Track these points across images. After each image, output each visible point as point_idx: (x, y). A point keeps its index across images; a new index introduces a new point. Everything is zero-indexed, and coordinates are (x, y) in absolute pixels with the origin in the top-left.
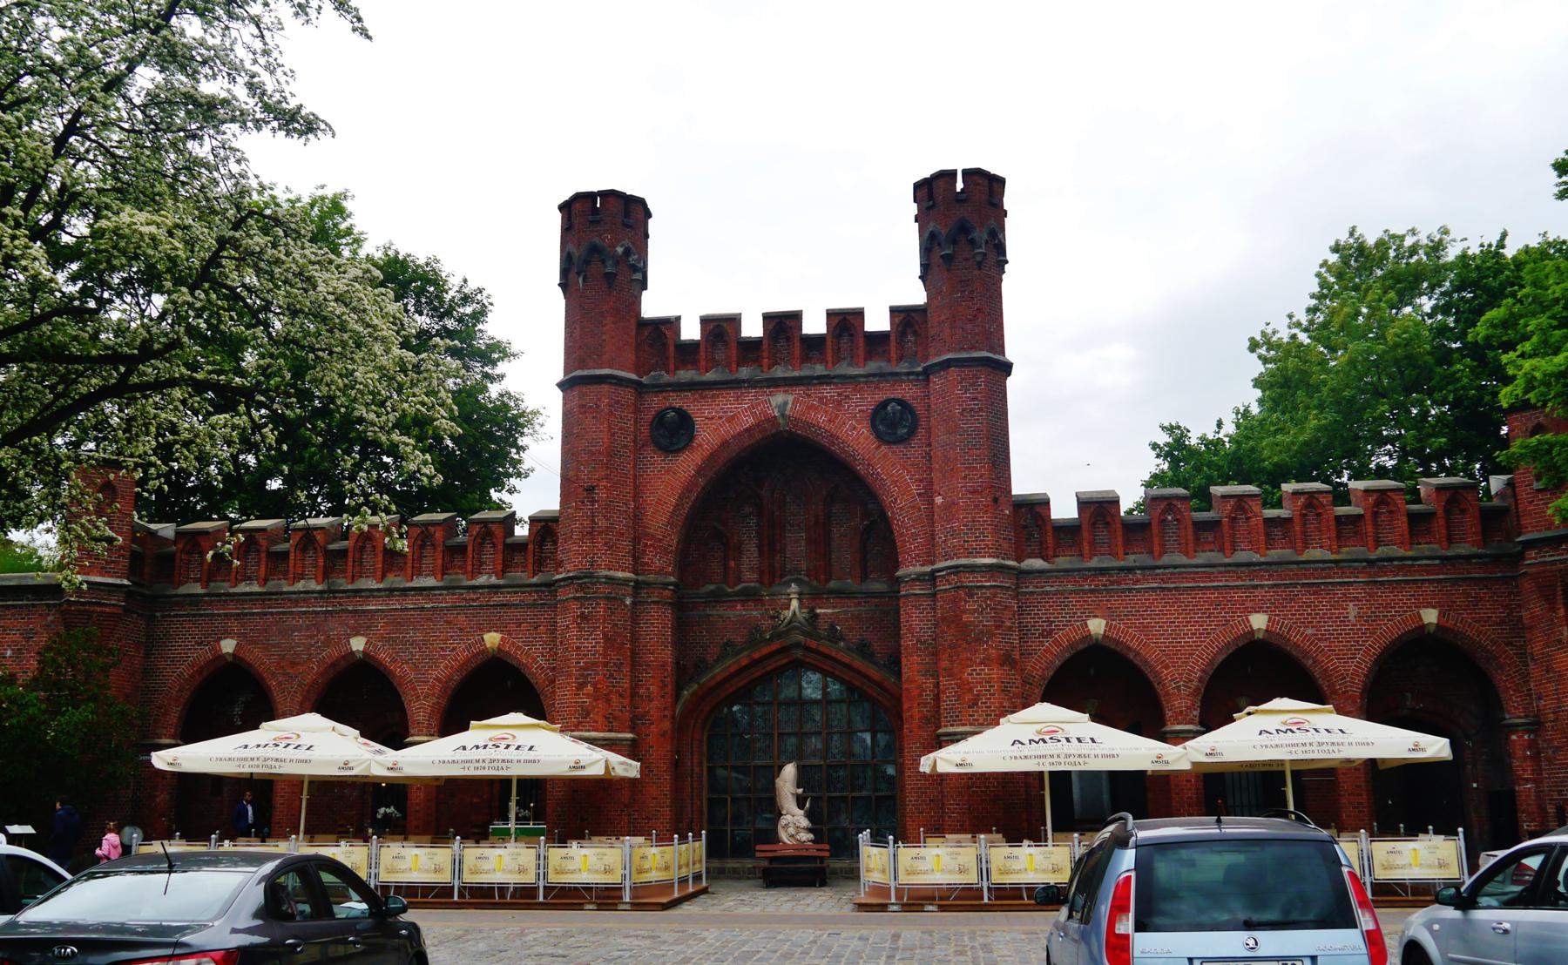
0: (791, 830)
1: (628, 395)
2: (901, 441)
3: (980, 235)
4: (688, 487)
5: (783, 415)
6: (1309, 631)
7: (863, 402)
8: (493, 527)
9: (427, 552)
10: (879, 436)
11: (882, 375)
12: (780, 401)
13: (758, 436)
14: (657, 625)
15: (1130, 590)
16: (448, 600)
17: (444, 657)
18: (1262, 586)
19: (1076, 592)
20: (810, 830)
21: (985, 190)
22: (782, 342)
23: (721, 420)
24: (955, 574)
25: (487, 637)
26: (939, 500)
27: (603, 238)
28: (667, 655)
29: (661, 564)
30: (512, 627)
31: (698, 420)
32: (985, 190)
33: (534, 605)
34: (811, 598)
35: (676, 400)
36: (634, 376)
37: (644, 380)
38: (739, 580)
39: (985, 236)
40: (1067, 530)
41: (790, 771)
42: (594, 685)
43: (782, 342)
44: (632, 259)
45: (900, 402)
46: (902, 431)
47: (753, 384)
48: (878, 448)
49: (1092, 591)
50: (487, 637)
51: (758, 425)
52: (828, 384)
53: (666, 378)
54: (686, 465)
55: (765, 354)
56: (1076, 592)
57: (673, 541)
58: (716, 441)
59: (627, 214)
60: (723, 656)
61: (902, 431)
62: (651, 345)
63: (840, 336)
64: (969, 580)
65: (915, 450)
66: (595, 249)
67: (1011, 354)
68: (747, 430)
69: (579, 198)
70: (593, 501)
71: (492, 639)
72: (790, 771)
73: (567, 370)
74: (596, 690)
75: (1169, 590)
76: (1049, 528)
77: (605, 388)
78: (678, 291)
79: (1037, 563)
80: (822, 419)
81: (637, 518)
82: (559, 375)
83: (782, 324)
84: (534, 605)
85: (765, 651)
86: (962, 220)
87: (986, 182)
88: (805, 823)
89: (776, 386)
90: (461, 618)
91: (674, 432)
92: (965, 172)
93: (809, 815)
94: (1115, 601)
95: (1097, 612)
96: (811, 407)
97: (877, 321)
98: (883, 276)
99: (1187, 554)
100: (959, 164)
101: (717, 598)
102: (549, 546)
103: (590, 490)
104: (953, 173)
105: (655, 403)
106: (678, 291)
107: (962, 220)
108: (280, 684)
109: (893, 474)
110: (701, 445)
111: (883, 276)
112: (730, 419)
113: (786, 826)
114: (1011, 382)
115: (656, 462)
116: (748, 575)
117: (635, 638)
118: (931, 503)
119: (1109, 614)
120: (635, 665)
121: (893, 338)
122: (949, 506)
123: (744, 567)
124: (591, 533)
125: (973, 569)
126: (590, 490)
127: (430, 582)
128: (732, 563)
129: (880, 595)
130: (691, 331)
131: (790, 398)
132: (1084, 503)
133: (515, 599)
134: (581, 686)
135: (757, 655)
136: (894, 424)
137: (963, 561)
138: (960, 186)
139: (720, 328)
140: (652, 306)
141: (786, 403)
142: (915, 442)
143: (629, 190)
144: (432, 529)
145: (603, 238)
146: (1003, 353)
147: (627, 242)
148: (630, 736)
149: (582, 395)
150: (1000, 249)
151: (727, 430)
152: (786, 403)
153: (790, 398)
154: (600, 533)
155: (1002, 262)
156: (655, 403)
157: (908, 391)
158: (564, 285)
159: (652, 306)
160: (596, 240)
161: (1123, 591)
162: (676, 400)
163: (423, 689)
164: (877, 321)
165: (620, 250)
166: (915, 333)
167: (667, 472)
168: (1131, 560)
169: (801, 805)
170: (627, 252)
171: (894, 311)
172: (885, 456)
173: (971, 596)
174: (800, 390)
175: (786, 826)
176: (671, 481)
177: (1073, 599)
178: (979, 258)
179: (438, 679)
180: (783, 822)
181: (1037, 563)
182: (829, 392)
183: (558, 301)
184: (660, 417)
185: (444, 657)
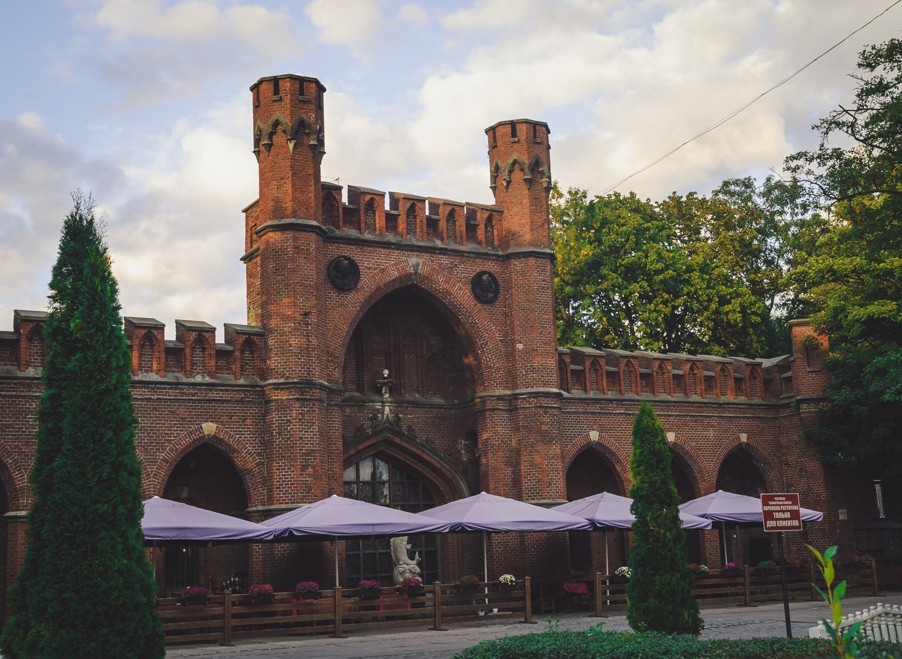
2: (491, 302)
5: (416, 273)
6: (694, 444)
10: (478, 297)
11: (478, 255)
12: (413, 260)
13: (397, 286)
15: (610, 413)
16: (172, 394)
17: (169, 442)
18: (672, 416)
19: (584, 413)
20: (420, 575)
23: (380, 269)
24: (534, 397)
25: (204, 425)
26: (520, 346)
33: (242, 401)
34: (399, 404)
35: (346, 251)
42: (314, 467)
45: (491, 275)
47: (399, 247)
48: (476, 305)
49: (592, 413)
50: (204, 425)
51: (400, 278)
52: (444, 254)
56: (584, 413)
61: (490, 295)
64: (545, 402)
65: (498, 308)
68: (393, 280)
71: (209, 428)
74: (315, 471)
75: (629, 415)
84: (242, 401)
89: (412, 251)
90: (181, 411)
91: (343, 275)
94: (604, 420)
95: (594, 427)
96: (433, 270)
99: (637, 394)
103: (306, 314)
108: (15, 462)
109: (484, 324)
110: (363, 288)
119: (601, 430)
122: (530, 351)
124: (307, 349)
125: (547, 395)
127: (153, 377)
129: (439, 406)
131: (421, 261)
133: (227, 396)
134: (304, 468)
135: (361, 447)
136: (486, 289)
137: (541, 389)
141: (418, 265)
149: (295, 239)
152: (418, 265)
153: (421, 261)
154: (313, 351)
157: (492, 267)
161: (607, 414)
162: (346, 251)
163: (151, 469)
167: (340, 306)
168: (610, 395)
169: (411, 556)
172: (480, 311)
173: (546, 413)
174: (426, 256)
177: (582, 417)
182: (445, 260)
185: (169, 442)
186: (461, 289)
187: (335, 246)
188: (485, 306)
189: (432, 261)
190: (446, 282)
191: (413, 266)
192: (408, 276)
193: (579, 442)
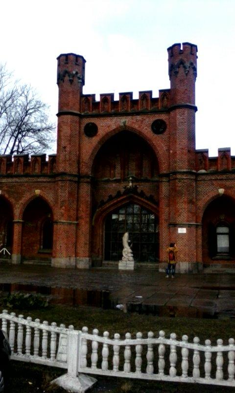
0: (126, 253)
1: (76, 118)
2: (162, 132)
3: (187, 64)
4: (95, 148)
5: (125, 125)
7: (150, 120)
8: (38, 158)
9: (20, 165)
13: (117, 132)
14: (85, 190)
20: (132, 253)
21: (191, 49)
22: (125, 102)
23: (107, 125)
25: (36, 191)
26: (171, 152)
27: (71, 69)
28: (89, 199)
29: (86, 170)
30: (43, 189)
31: (99, 127)
32: (191, 49)
33: (49, 182)
36: (79, 113)
37: (83, 114)
38: (114, 176)
39: (189, 65)
40: (214, 160)
41: (126, 235)
43: (125, 102)
44: (79, 75)
46: (161, 130)
50: (36, 191)
53: (90, 113)
54: (95, 140)
55: (120, 106)
57: (91, 163)
58: (104, 133)
59: (77, 61)
60: (108, 201)
61: (161, 130)
62: (85, 103)
63: (143, 100)
65: (165, 136)
66: (66, 72)
67: (197, 104)
68: (114, 130)
69: (61, 55)
70: (65, 151)
71: (38, 192)
72: (126, 235)
73: (60, 109)
76: (207, 160)
77: (69, 116)
78: (95, 85)
79: (203, 171)
80: (136, 126)
81: (79, 157)
82: (57, 112)
83: (126, 96)
85: (122, 198)
86: (183, 60)
87: (190, 47)
88: (130, 251)
91: (91, 130)
92: (184, 44)
93: (131, 248)
94: (228, 183)
97: (156, 95)
98: (156, 80)
100: (181, 41)
101: (108, 181)
102: (55, 164)
104: (179, 45)
105: (86, 121)
106: (95, 85)
107: (183, 60)
109: (159, 143)
111: (156, 80)
112: (109, 127)
113: (125, 252)
114: (197, 114)
115: (86, 140)
116: (117, 175)
117: (78, 193)
118: (170, 152)
120: (78, 201)
121: (159, 100)
123: (116, 173)
126: (65, 147)
128: (112, 171)
130: (98, 99)
131: (127, 120)
132: (220, 151)
134: (61, 207)
136: (159, 127)
138: (182, 49)
139: (107, 98)
140: (86, 91)
141: (125, 122)
142: (165, 133)
143: (77, 53)
144: (20, 158)
145: (71, 69)
146: (194, 103)
147: (77, 70)
148: (76, 222)
150: (195, 69)
151: (108, 130)
153: (127, 120)
155: (195, 75)
156: (86, 121)
157: (163, 117)
158: (58, 83)
159: (86, 91)
160: (67, 70)
164: (156, 95)
165: (74, 72)
166: (167, 98)
170: (77, 73)
171: (160, 91)
172: (156, 138)
175: (125, 252)
176: (90, 145)
177: (214, 182)
178: (187, 72)
179: (22, 203)
180: (124, 250)
181: (203, 171)
182: (139, 118)
183: (56, 89)
184: (88, 125)
186: (146, 129)
187: (88, 119)
188: (159, 135)
189: (133, 119)
190: (139, 127)
191: (123, 123)
192: (121, 127)
193: (212, 194)
